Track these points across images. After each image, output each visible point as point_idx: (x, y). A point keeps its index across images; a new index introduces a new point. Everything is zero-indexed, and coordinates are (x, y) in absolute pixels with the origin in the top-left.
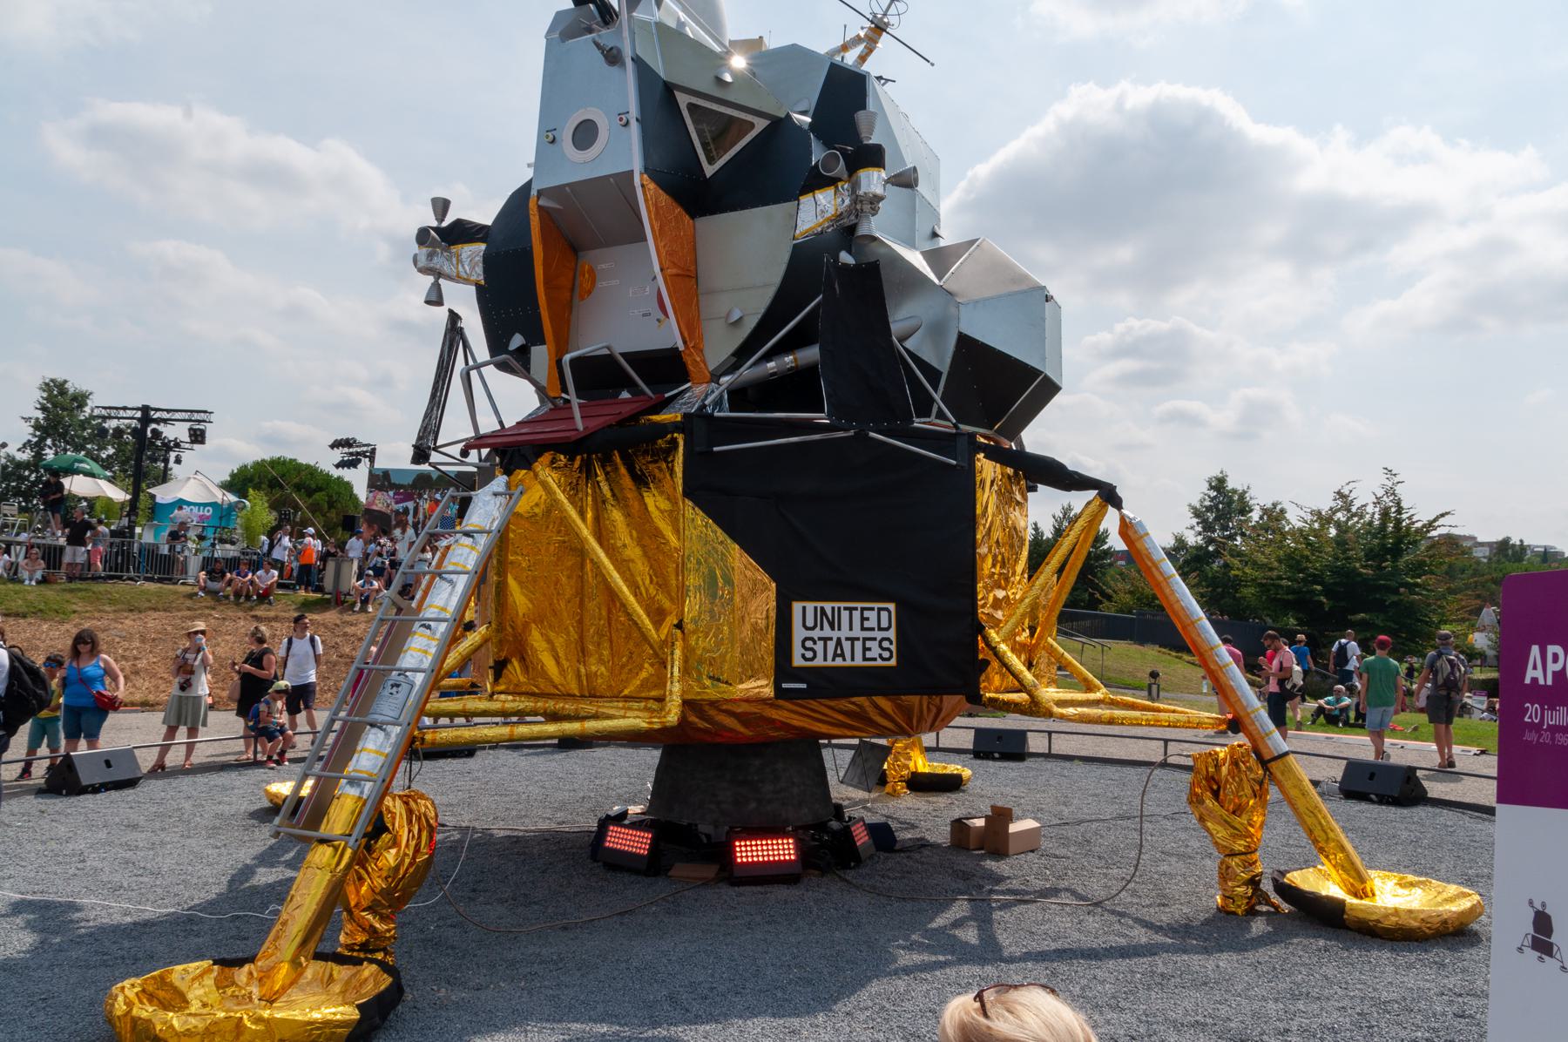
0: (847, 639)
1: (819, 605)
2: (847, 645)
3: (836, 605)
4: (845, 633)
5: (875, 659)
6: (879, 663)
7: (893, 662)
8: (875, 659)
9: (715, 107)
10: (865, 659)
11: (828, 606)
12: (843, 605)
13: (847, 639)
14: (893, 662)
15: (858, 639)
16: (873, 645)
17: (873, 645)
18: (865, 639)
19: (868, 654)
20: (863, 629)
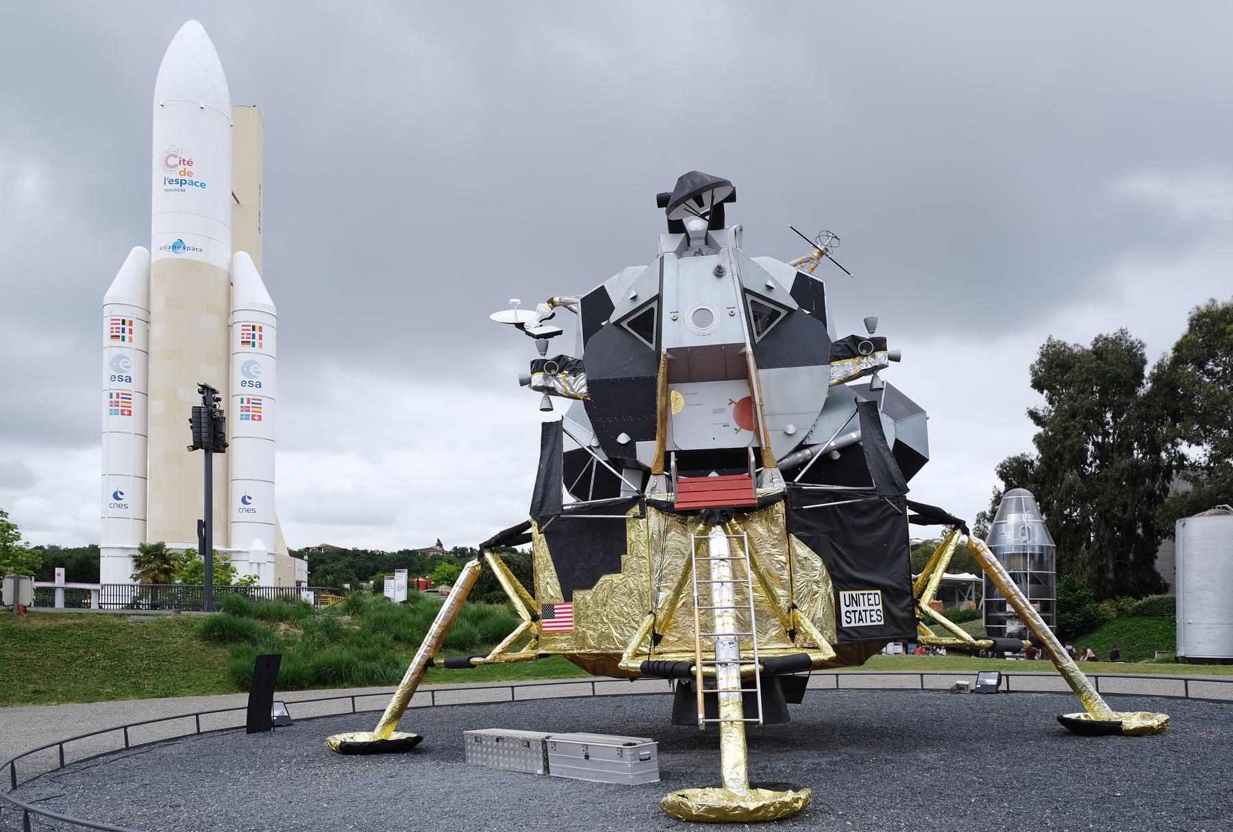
0: (863, 611)
1: (850, 592)
2: (863, 613)
3: (858, 592)
4: (862, 608)
5: (875, 621)
6: (877, 623)
7: (882, 623)
8: (875, 621)
9: (763, 303)
10: (871, 621)
11: (854, 593)
12: (860, 592)
13: (863, 611)
14: (882, 623)
15: (867, 611)
16: (873, 613)
17: (873, 613)
18: (871, 610)
19: (873, 619)
20: (869, 605)
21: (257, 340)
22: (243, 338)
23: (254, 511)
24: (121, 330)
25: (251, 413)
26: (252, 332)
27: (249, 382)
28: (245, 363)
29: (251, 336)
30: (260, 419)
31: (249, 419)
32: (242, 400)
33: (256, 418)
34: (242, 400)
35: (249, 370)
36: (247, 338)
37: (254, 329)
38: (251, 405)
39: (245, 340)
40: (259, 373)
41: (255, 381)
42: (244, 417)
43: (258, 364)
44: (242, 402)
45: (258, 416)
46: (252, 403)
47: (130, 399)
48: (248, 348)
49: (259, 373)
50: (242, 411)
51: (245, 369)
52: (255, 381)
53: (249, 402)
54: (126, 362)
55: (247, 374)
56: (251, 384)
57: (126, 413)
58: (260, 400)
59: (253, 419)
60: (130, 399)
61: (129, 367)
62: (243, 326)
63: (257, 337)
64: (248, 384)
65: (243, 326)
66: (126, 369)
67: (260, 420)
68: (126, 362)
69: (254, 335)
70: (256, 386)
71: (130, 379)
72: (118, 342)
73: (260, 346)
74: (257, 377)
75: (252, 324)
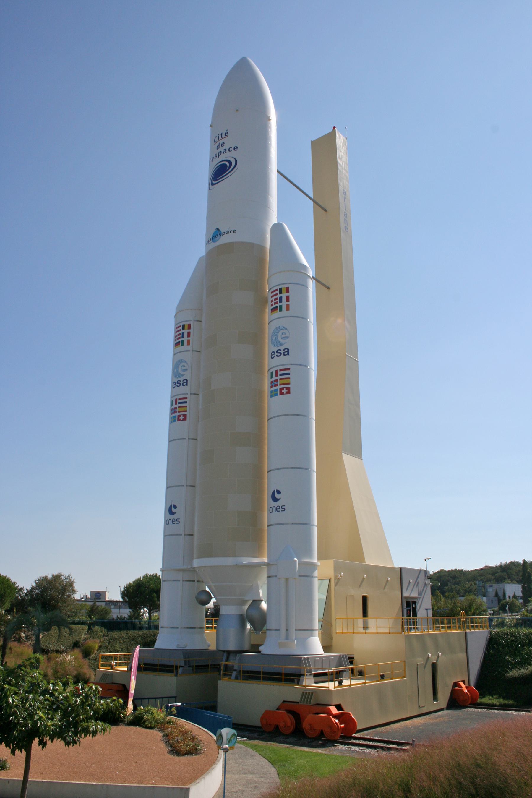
21: (284, 303)
22: (272, 305)
23: (283, 508)
24: (181, 336)
25: (279, 387)
26: (279, 296)
27: (277, 352)
28: (274, 332)
29: (278, 300)
30: (288, 392)
31: (276, 395)
32: (272, 373)
33: (285, 391)
34: (272, 373)
35: (277, 338)
36: (275, 303)
37: (281, 292)
38: (279, 377)
39: (274, 306)
40: (287, 338)
41: (282, 348)
42: (273, 393)
43: (287, 330)
44: (272, 377)
45: (287, 388)
46: (281, 375)
47: (186, 402)
48: (277, 314)
49: (287, 338)
50: (271, 387)
51: (274, 338)
52: (282, 348)
53: (277, 375)
54: (184, 366)
55: (276, 343)
56: (279, 353)
57: (182, 418)
58: (289, 369)
59: (282, 393)
60: (186, 402)
61: (186, 370)
62: (272, 293)
63: (284, 299)
64: (276, 354)
65: (272, 293)
66: (182, 373)
67: (288, 392)
68: (184, 366)
69: (281, 298)
70: (284, 355)
71: (187, 382)
72: (180, 348)
73: (288, 308)
74: (283, 344)
75: (278, 287)
